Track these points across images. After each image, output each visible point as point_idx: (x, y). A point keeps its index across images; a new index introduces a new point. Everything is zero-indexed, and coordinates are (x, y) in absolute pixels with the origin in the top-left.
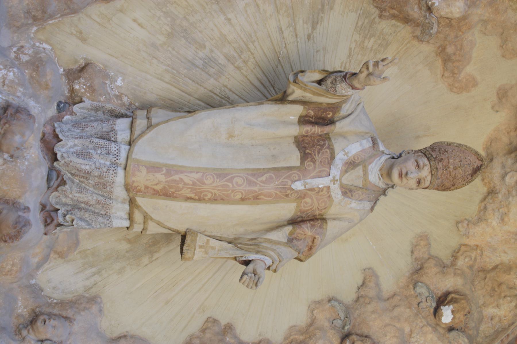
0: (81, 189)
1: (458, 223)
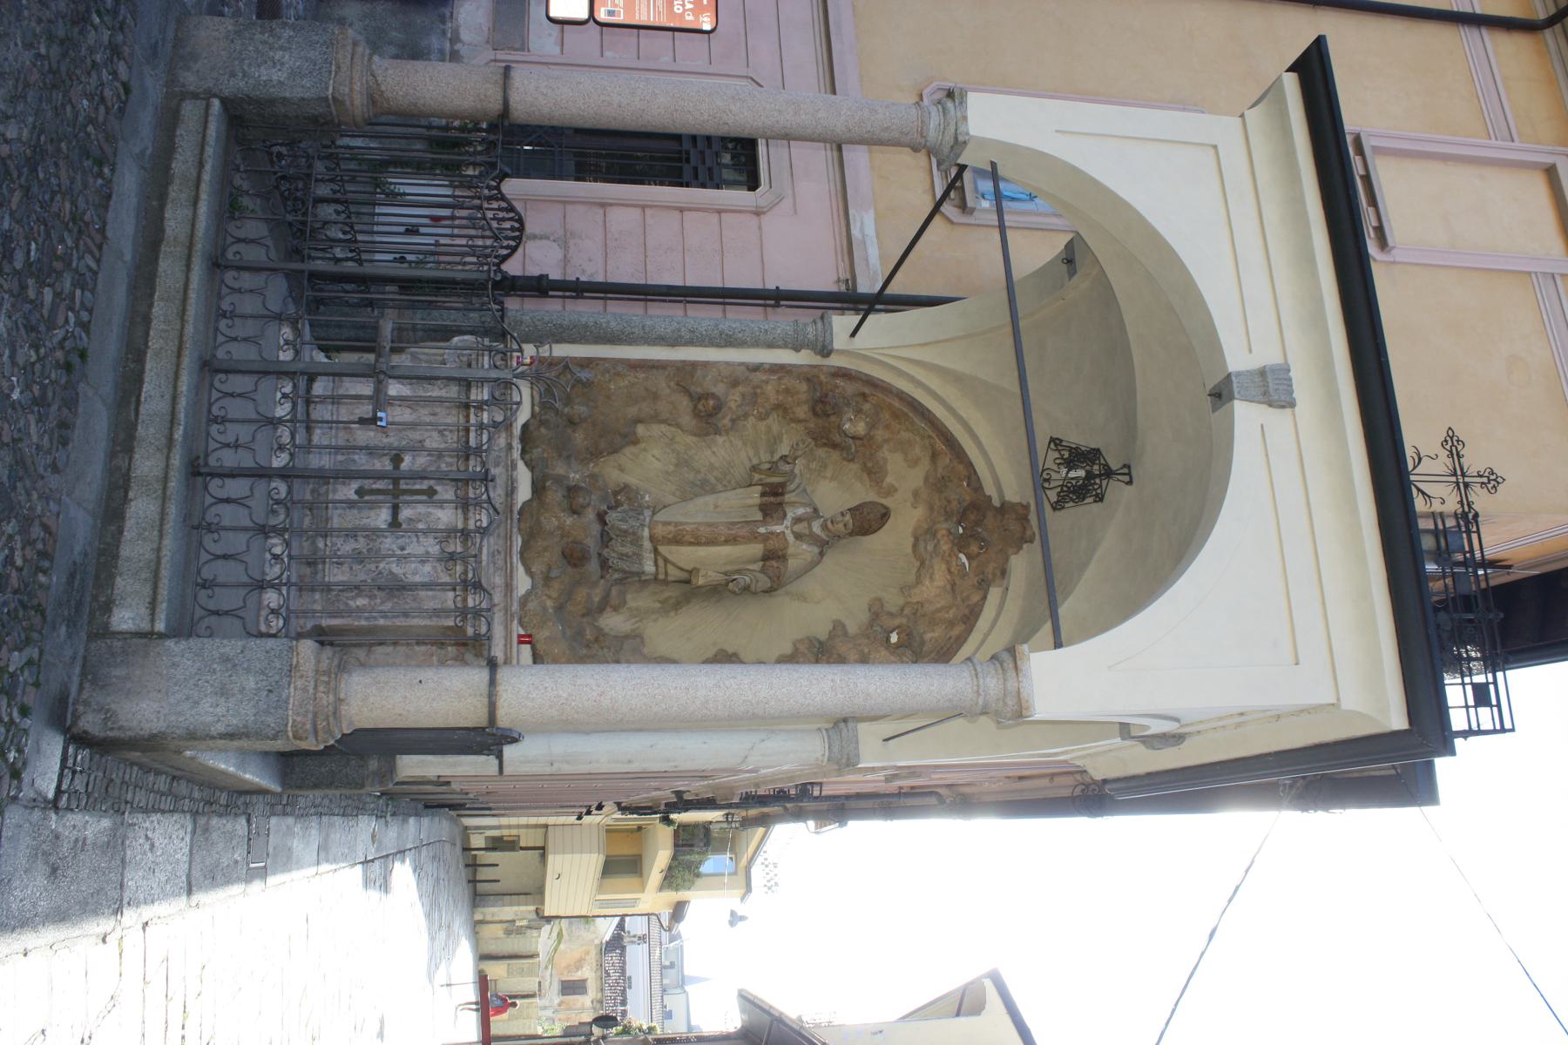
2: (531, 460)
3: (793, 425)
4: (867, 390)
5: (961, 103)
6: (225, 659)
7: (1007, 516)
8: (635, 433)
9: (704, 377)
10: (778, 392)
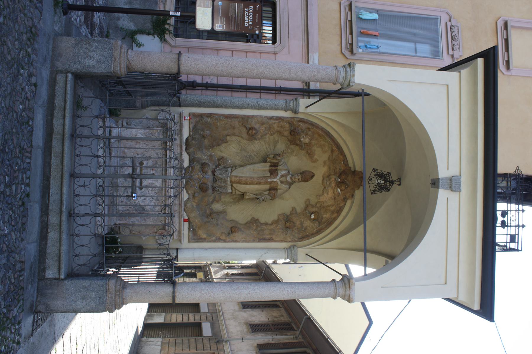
0: (220, 183)
1: (317, 196)
2: (189, 152)
3: (283, 137)
4: (310, 127)
5: (353, 69)
6: (85, 287)
8: (226, 139)
9: (252, 122)
10: (278, 127)
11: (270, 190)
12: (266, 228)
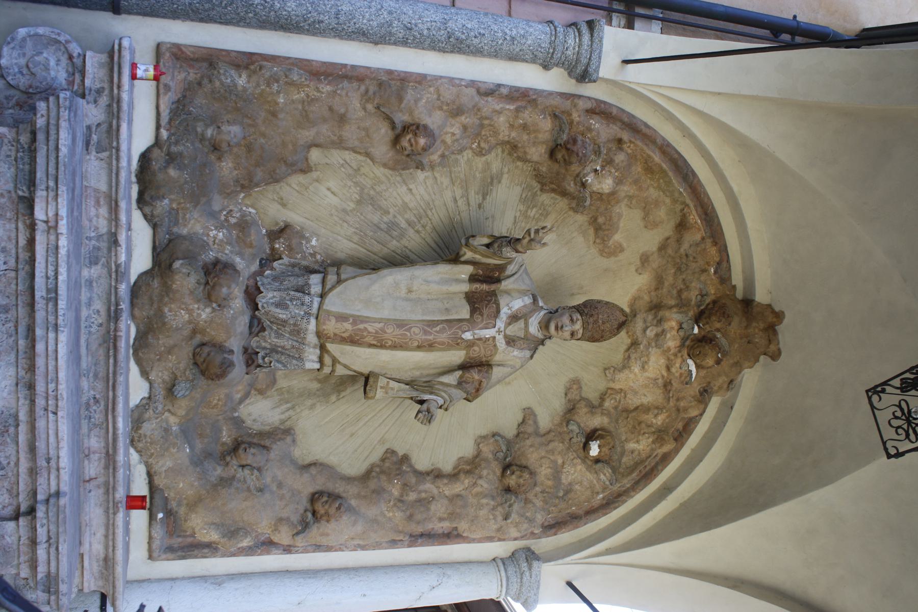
0: (279, 335)
1: (605, 369)
2: (152, 215)
3: (519, 164)
4: (625, 136)
7: (754, 324)
8: (307, 159)
9: (417, 101)
10: (512, 126)
11: (464, 367)
12: (435, 491)
